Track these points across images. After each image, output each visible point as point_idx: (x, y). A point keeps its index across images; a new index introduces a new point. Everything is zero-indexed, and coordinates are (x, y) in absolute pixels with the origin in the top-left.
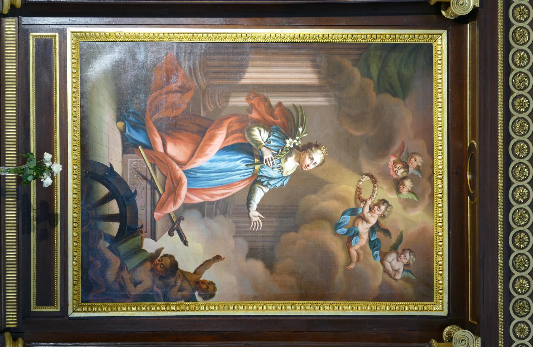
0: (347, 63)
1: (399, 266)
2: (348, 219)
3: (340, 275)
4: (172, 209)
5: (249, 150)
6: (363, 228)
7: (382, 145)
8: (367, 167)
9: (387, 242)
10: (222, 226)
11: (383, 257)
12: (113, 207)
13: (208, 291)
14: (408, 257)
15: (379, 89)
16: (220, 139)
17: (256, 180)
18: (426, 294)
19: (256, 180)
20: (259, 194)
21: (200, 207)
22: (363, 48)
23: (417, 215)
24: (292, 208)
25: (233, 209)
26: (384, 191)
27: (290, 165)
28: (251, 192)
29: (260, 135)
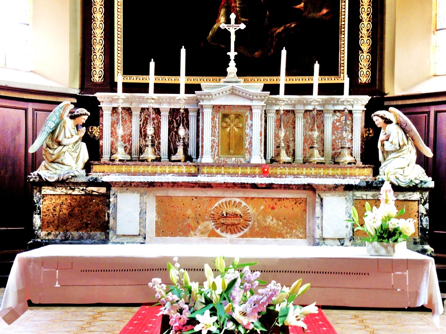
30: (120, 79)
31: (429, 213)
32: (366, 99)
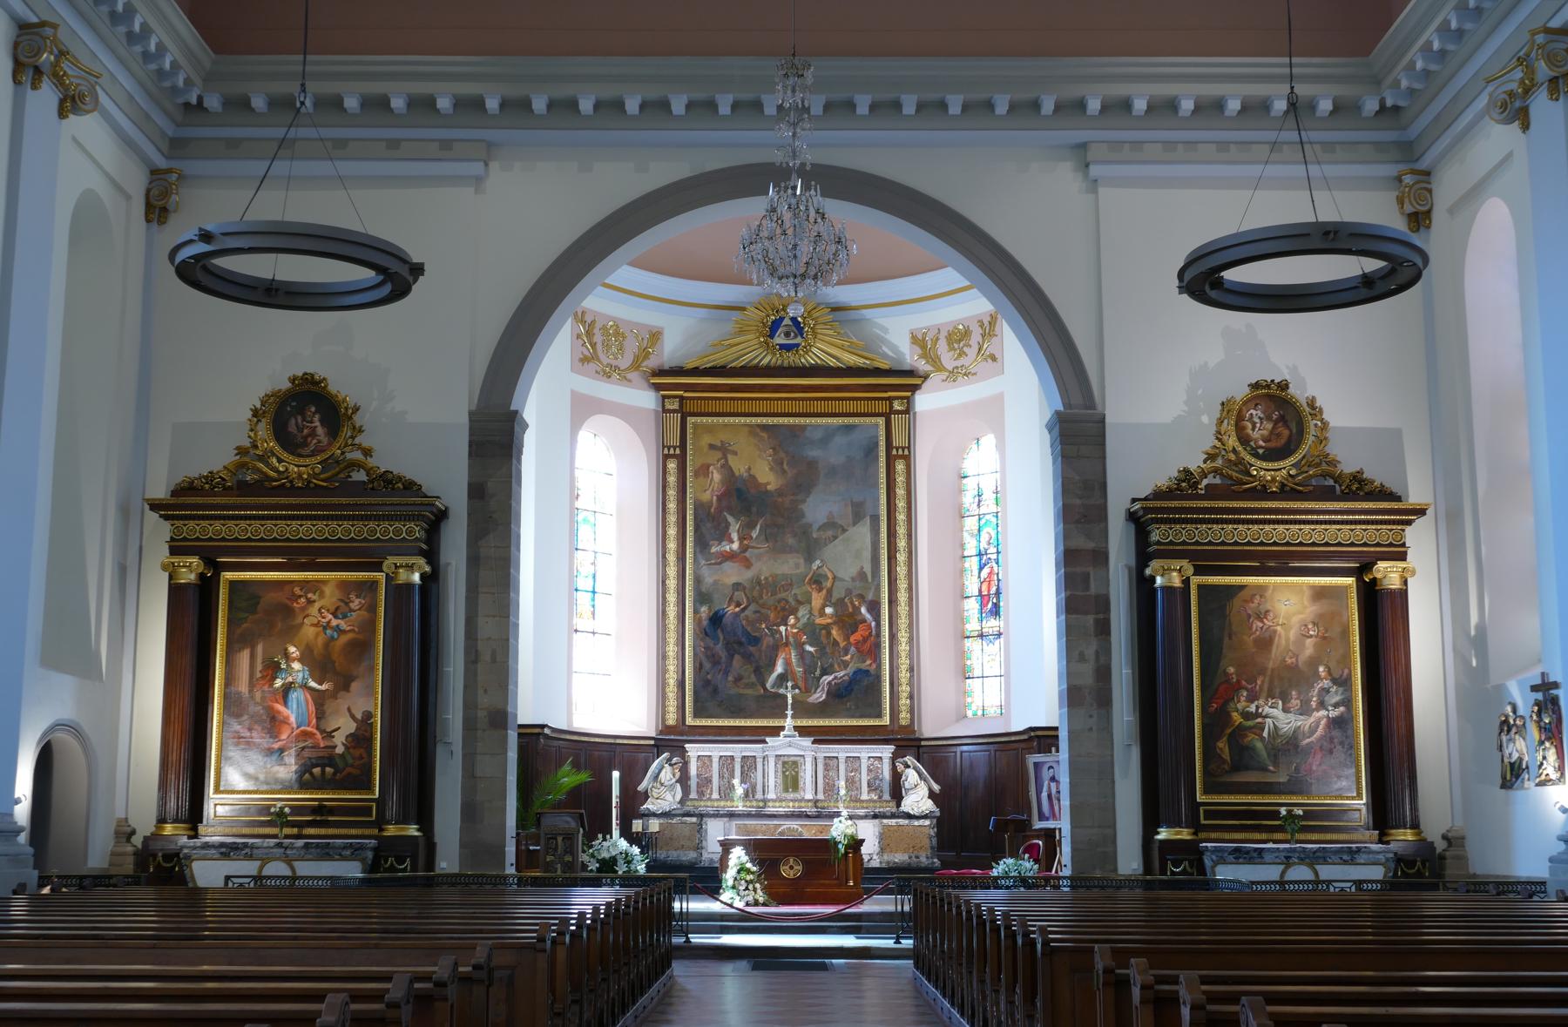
0: (239, 631)
1: (357, 601)
2: (329, 632)
3: (360, 637)
4: (319, 736)
5: (288, 688)
6: (334, 622)
7: (287, 611)
8: (299, 620)
9: (344, 608)
10: (330, 706)
11: (351, 610)
12: (317, 771)
13: (368, 715)
14: (352, 596)
15: (254, 612)
16: (280, 707)
17: (305, 686)
18: (373, 585)
19: (305, 686)
20: (313, 684)
21: (318, 719)
22: (231, 623)
23: (328, 590)
24: (320, 664)
25: (320, 699)
26: (314, 610)
27: (296, 666)
28: (311, 689)
29: (278, 683)
30: (690, 721)
31: (938, 834)
32: (891, 748)
